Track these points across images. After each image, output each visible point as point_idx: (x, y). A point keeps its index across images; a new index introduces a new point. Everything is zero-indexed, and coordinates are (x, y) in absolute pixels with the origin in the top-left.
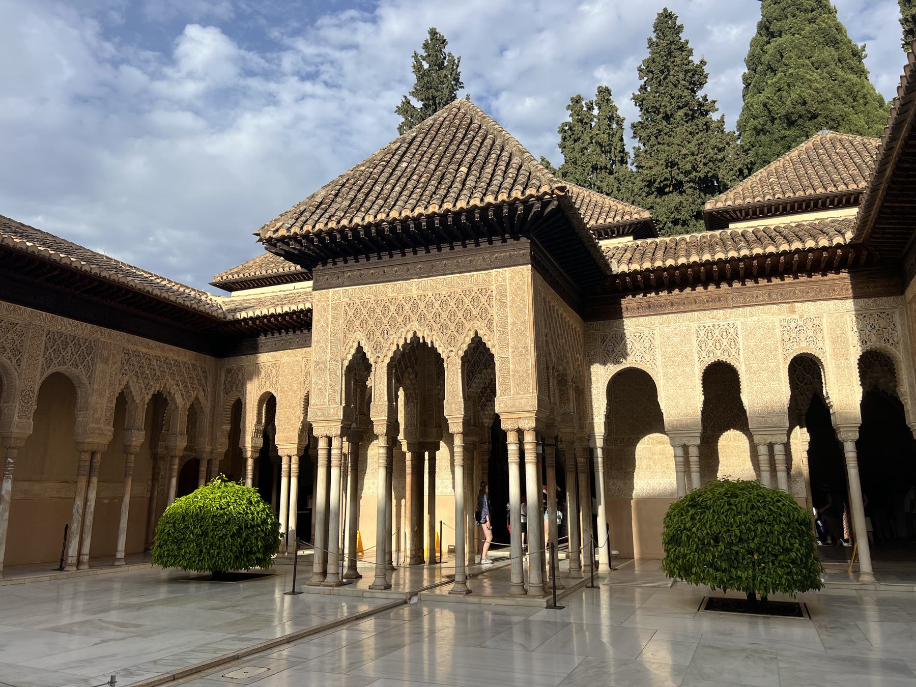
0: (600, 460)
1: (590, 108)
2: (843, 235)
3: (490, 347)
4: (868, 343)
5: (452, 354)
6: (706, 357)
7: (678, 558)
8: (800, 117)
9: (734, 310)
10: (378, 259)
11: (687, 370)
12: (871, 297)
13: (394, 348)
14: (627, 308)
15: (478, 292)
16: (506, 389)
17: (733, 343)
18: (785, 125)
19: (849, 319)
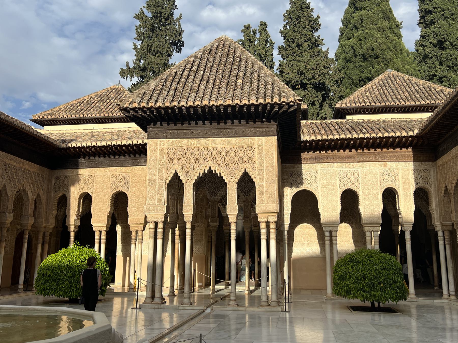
0: (286, 237)
1: (255, 33)
2: (413, 131)
3: (253, 178)
4: (419, 184)
5: (232, 180)
6: (343, 186)
7: (344, 286)
8: (370, 56)
9: (358, 163)
10: (188, 125)
11: (334, 192)
12: (422, 162)
13: (197, 175)
14: (304, 158)
15: (247, 149)
16: (262, 201)
17: (356, 180)
18: (362, 59)
19: (411, 172)
